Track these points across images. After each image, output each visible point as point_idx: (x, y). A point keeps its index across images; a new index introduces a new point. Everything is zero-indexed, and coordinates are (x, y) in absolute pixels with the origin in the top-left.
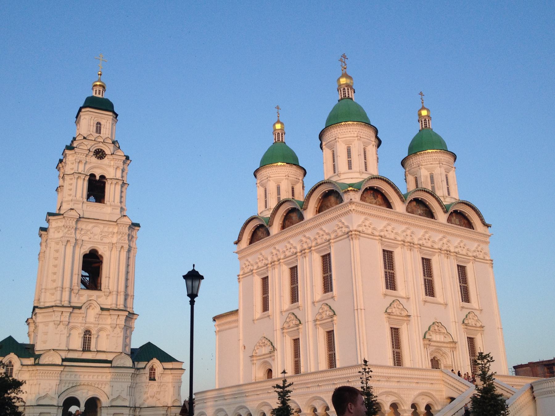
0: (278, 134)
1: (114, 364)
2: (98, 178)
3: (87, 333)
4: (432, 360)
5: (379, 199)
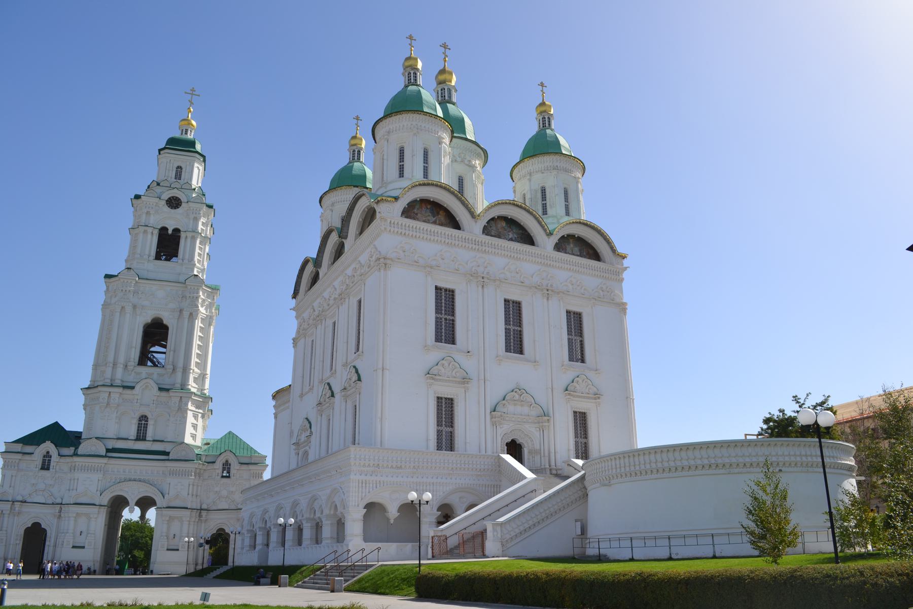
0: (354, 151)
1: (171, 457)
2: (170, 232)
3: (143, 419)
4: (507, 444)
5: (442, 217)
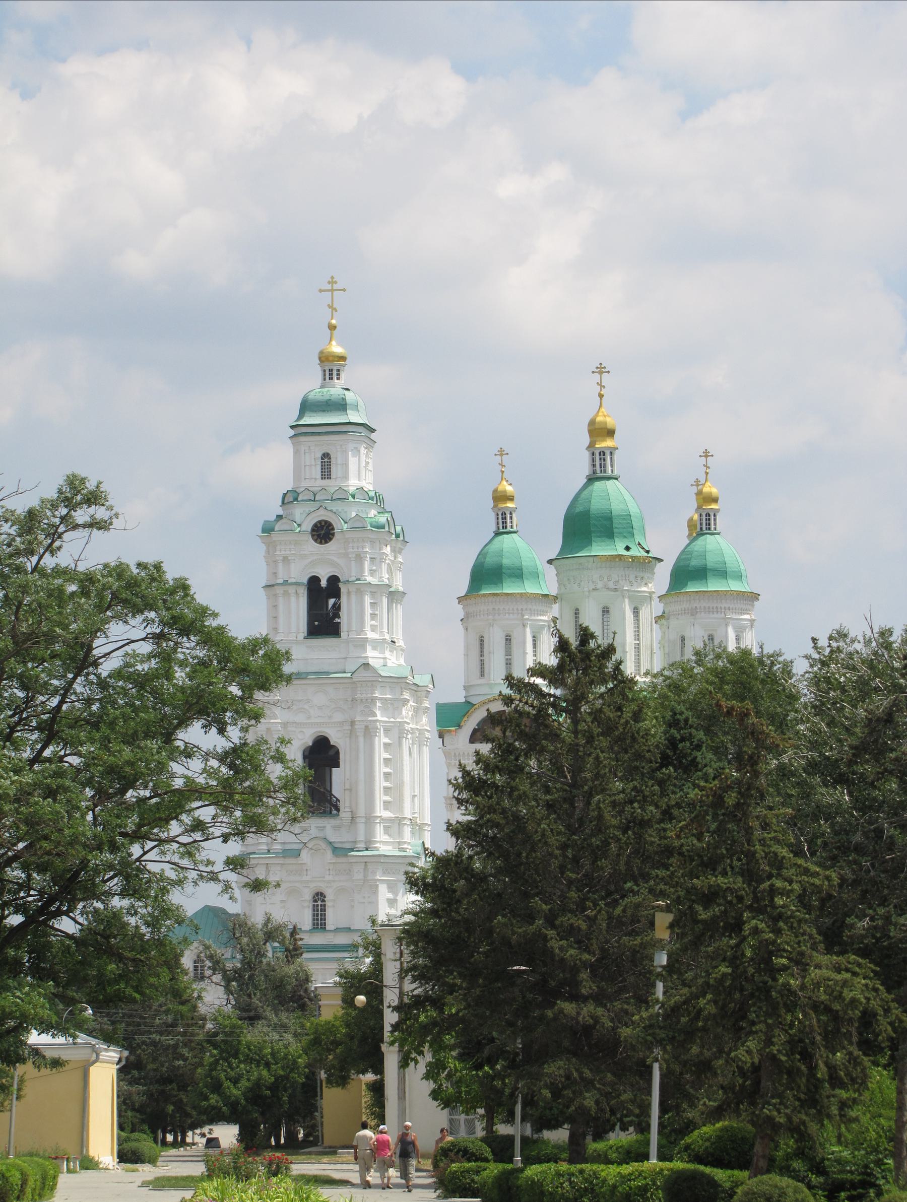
3: (319, 897)
